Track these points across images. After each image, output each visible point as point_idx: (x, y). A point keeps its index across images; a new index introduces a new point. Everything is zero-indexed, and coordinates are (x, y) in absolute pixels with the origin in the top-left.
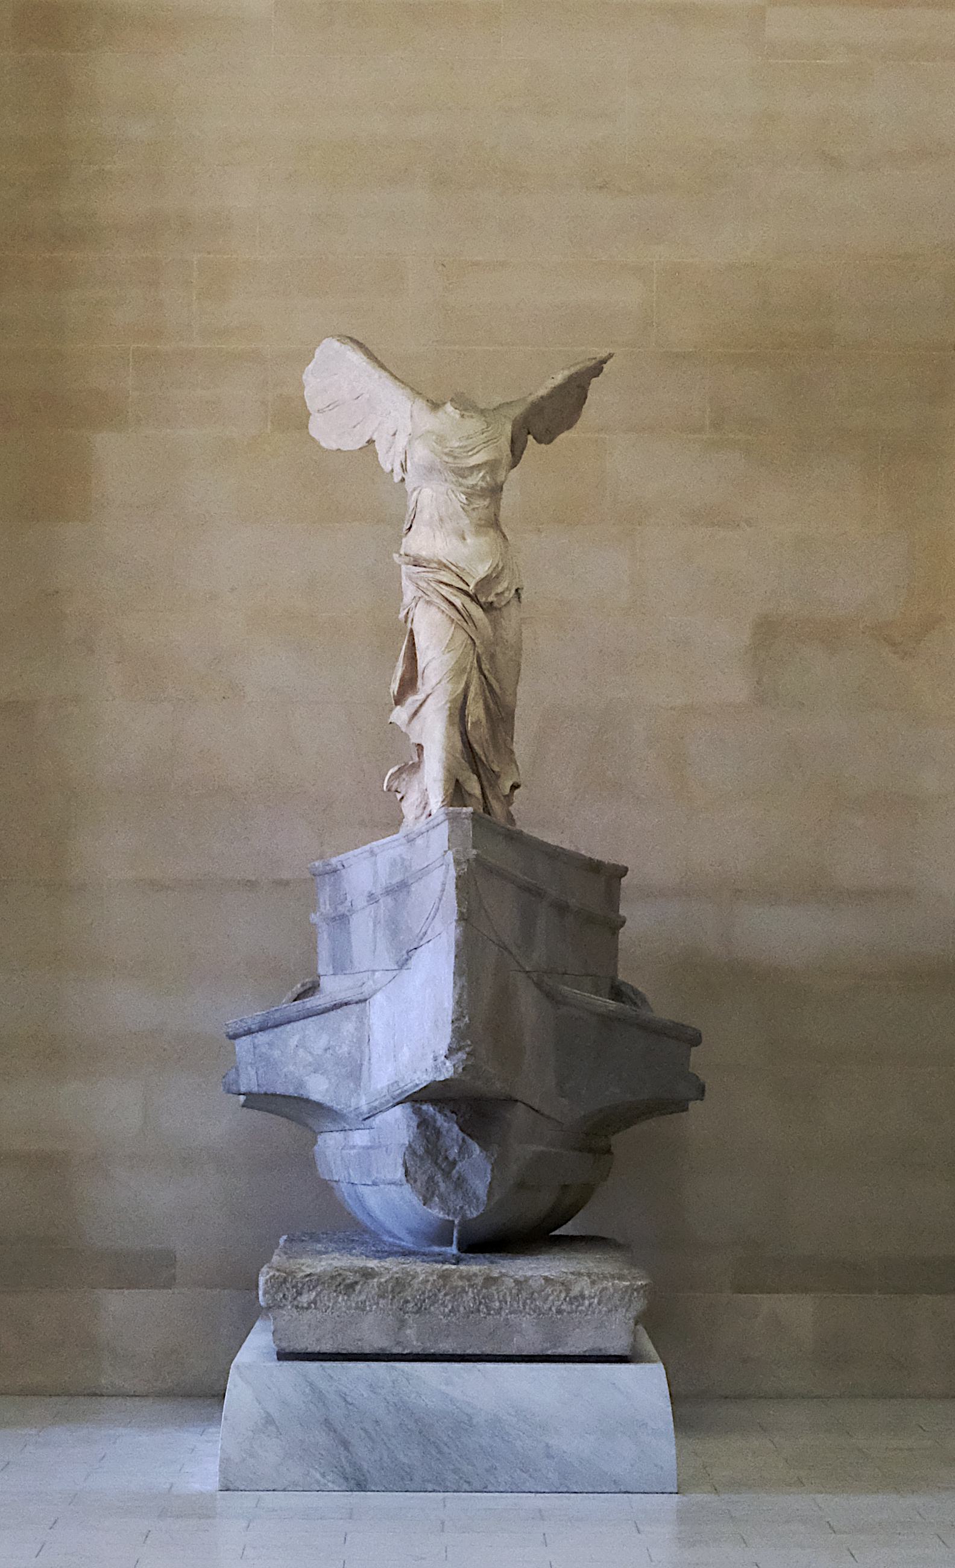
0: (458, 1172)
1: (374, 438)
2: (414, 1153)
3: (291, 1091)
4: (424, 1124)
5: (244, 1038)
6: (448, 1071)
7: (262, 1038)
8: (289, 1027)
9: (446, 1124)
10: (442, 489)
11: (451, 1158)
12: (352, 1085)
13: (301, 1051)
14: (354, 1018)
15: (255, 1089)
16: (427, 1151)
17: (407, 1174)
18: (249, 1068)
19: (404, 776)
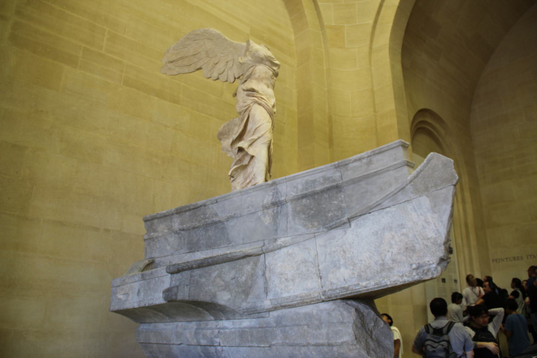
0: (375, 336)
1: (202, 67)
2: (356, 326)
3: (207, 299)
4: (357, 310)
5: (186, 272)
6: (437, 273)
7: (197, 272)
8: (213, 267)
9: (366, 311)
10: (266, 68)
11: (370, 329)
12: (243, 297)
13: (218, 280)
14: (252, 263)
15: (187, 298)
16: (362, 325)
17: (356, 339)
18: (186, 287)
19: (239, 170)
